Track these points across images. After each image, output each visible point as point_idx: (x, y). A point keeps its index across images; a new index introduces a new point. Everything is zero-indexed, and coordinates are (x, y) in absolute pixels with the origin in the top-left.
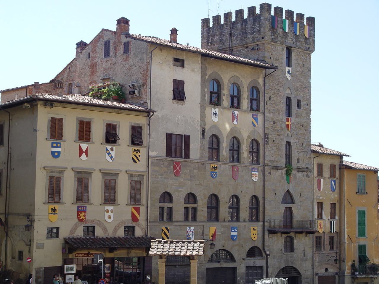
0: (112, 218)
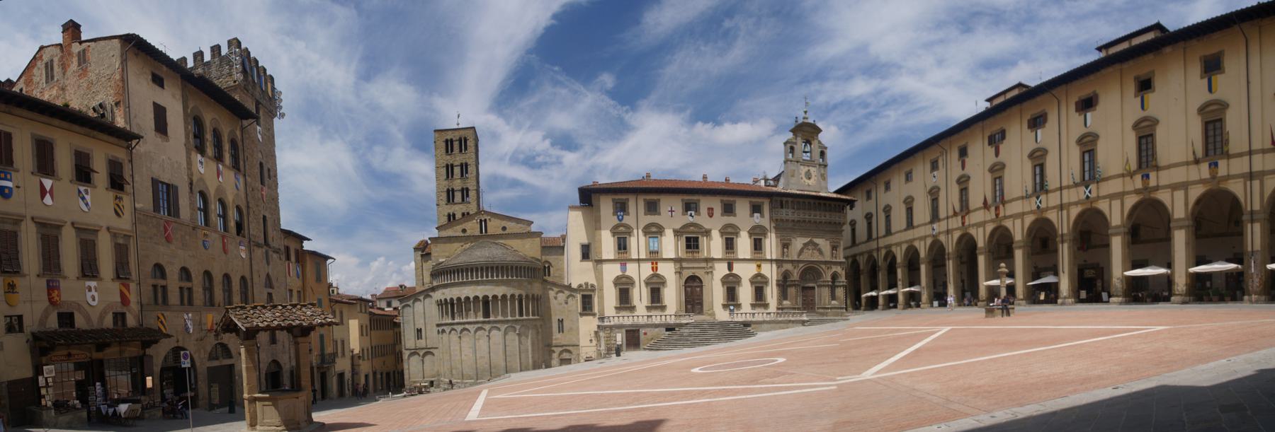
0: (97, 299)
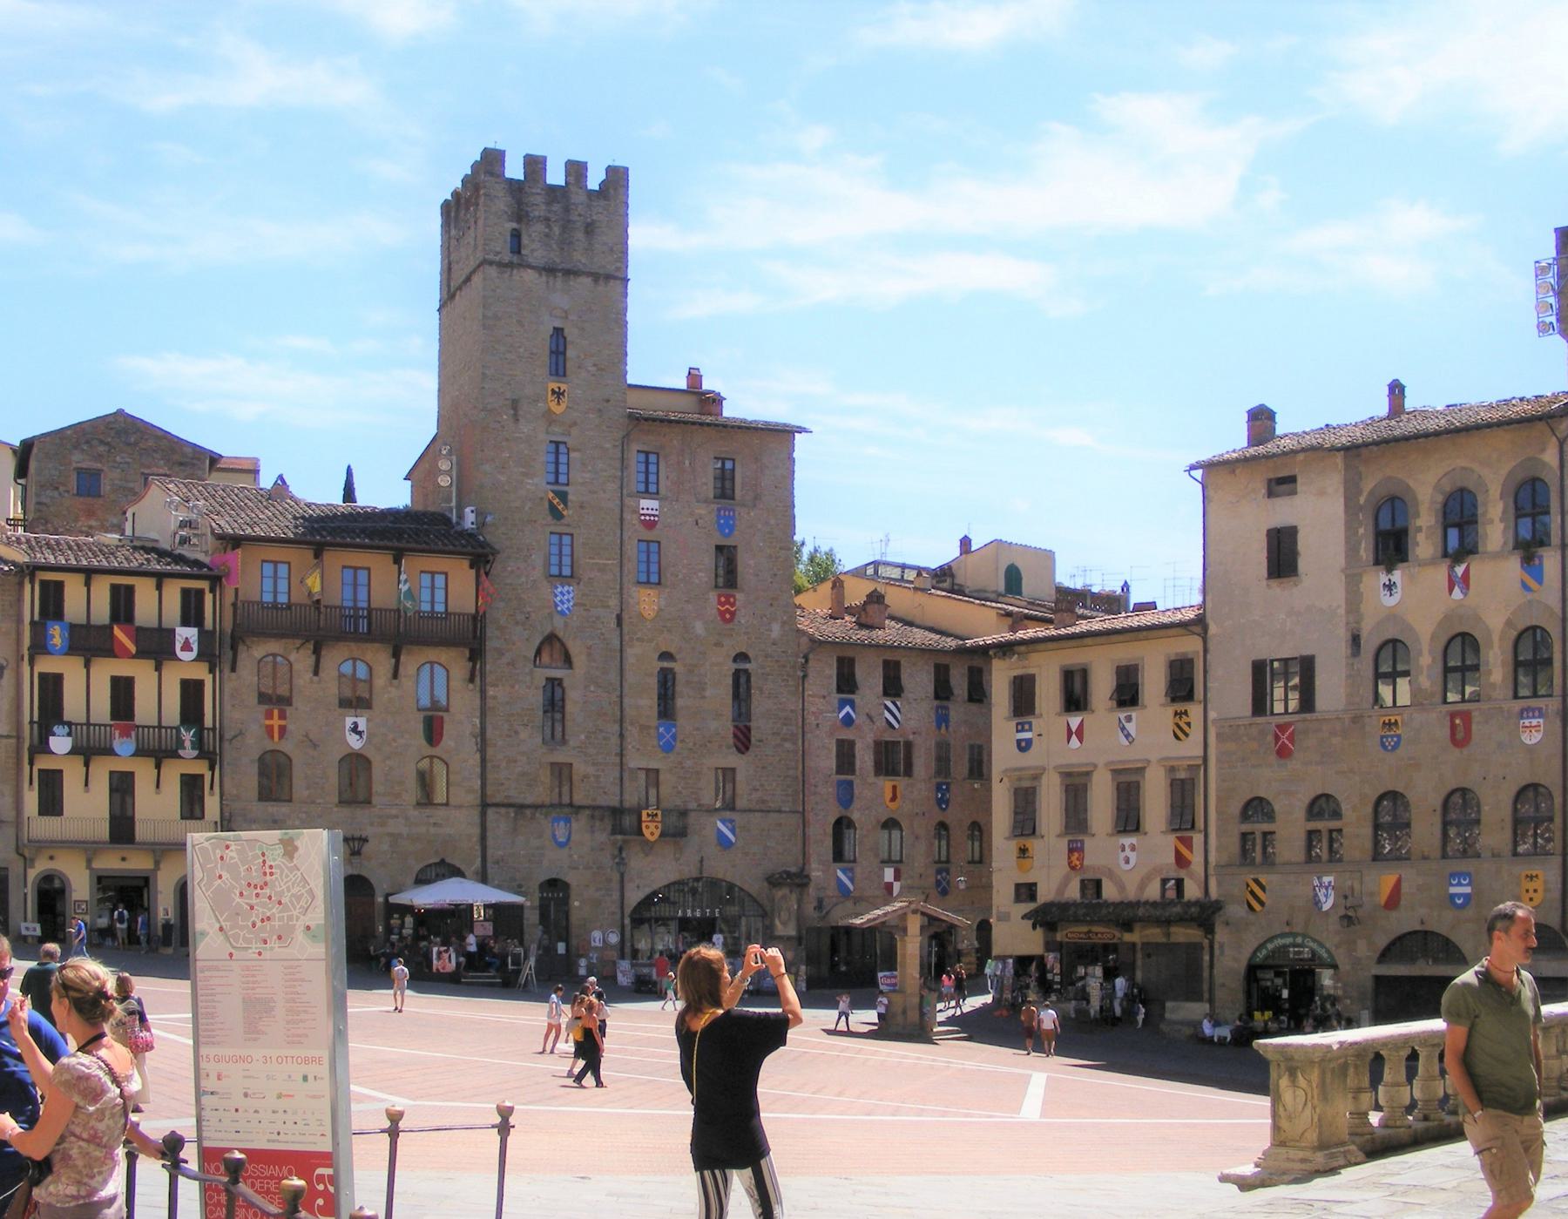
0: (1133, 862)
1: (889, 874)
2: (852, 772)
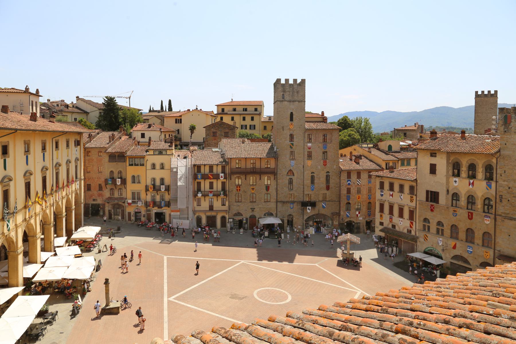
1: (357, 213)
2: (350, 194)
